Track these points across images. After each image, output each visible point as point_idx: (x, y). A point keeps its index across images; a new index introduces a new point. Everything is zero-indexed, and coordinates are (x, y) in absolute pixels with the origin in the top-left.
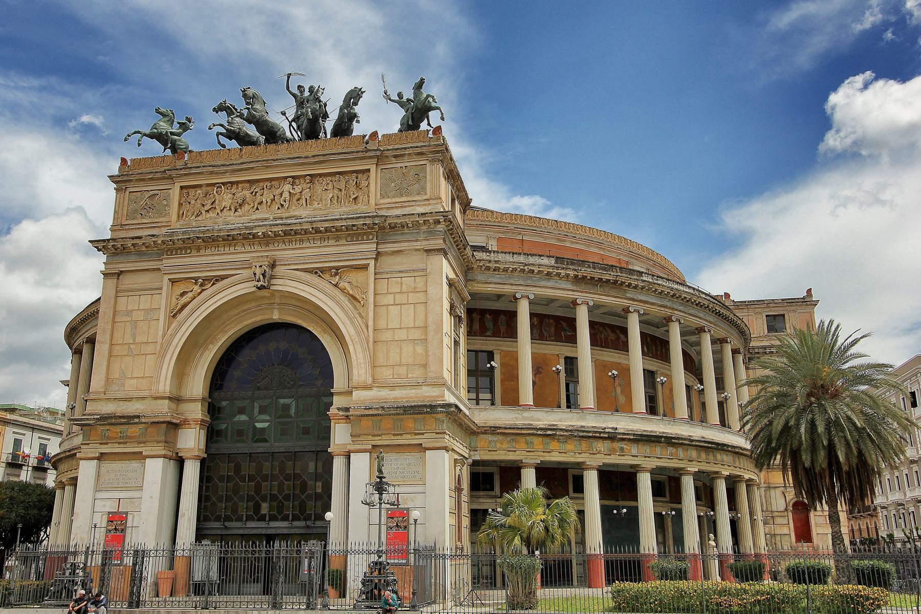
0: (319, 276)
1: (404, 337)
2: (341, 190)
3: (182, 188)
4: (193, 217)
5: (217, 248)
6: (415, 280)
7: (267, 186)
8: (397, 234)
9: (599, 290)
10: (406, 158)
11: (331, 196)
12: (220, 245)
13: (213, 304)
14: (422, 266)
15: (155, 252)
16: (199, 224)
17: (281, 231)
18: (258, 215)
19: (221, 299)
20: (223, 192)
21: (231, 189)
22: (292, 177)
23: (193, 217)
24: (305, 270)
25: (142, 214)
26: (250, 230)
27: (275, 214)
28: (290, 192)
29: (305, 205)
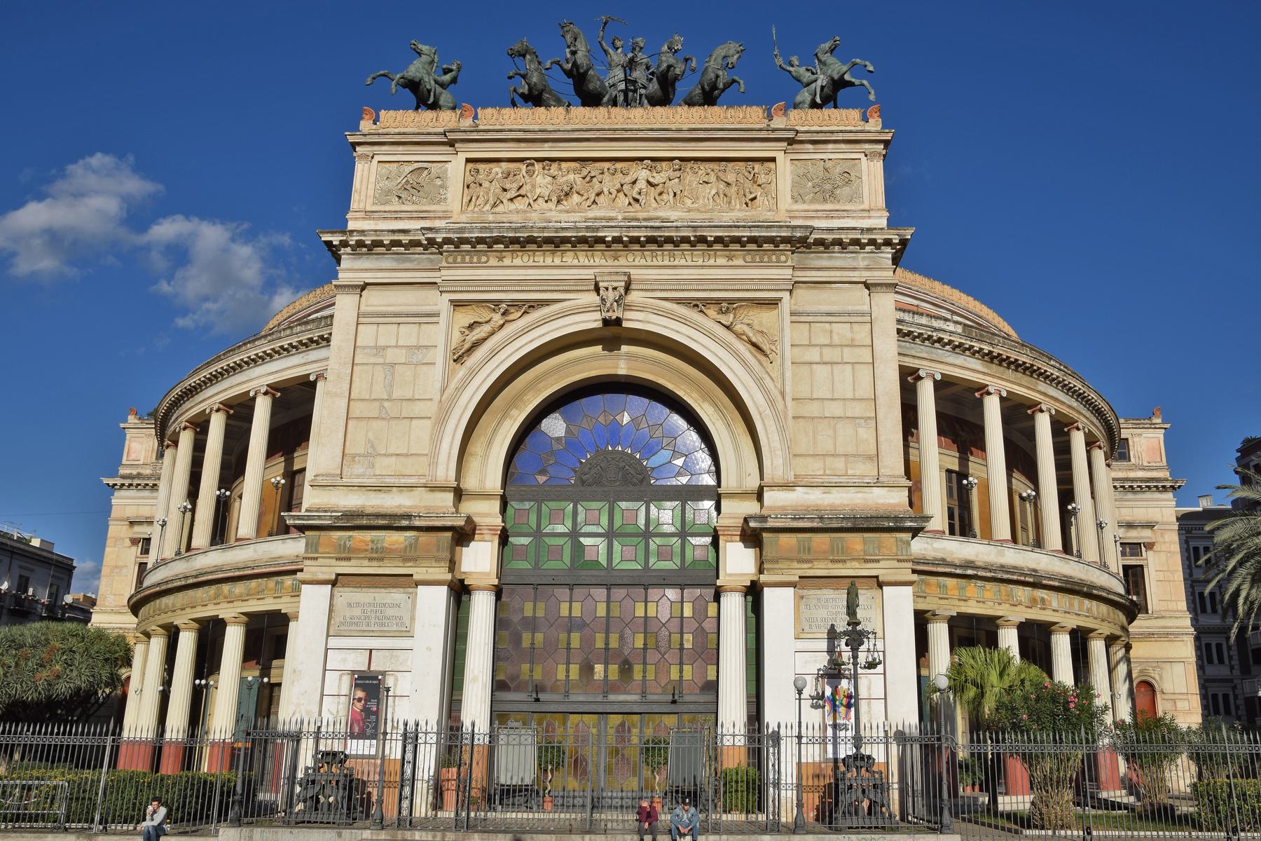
0: (701, 311)
1: (839, 413)
3: (468, 160)
4: (488, 207)
5: (532, 258)
6: (851, 328)
8: (821, 258)
9: (1010, 374)
10: (830, 146)
11: (714, 192)
12: (537, 253)
13: (526, 344)
14: (866, 308)
15: (425, 256)
16: (499, 218)
17: (644, 236)
18: (595, 212)
19: (540, 336)
20: (536, 173)
22: (653, 159)
23: (488, 207)
24: (679, 301)
25: (399, 197)
26: (593, 232)
27: (626, 212)
28: (648, 182)
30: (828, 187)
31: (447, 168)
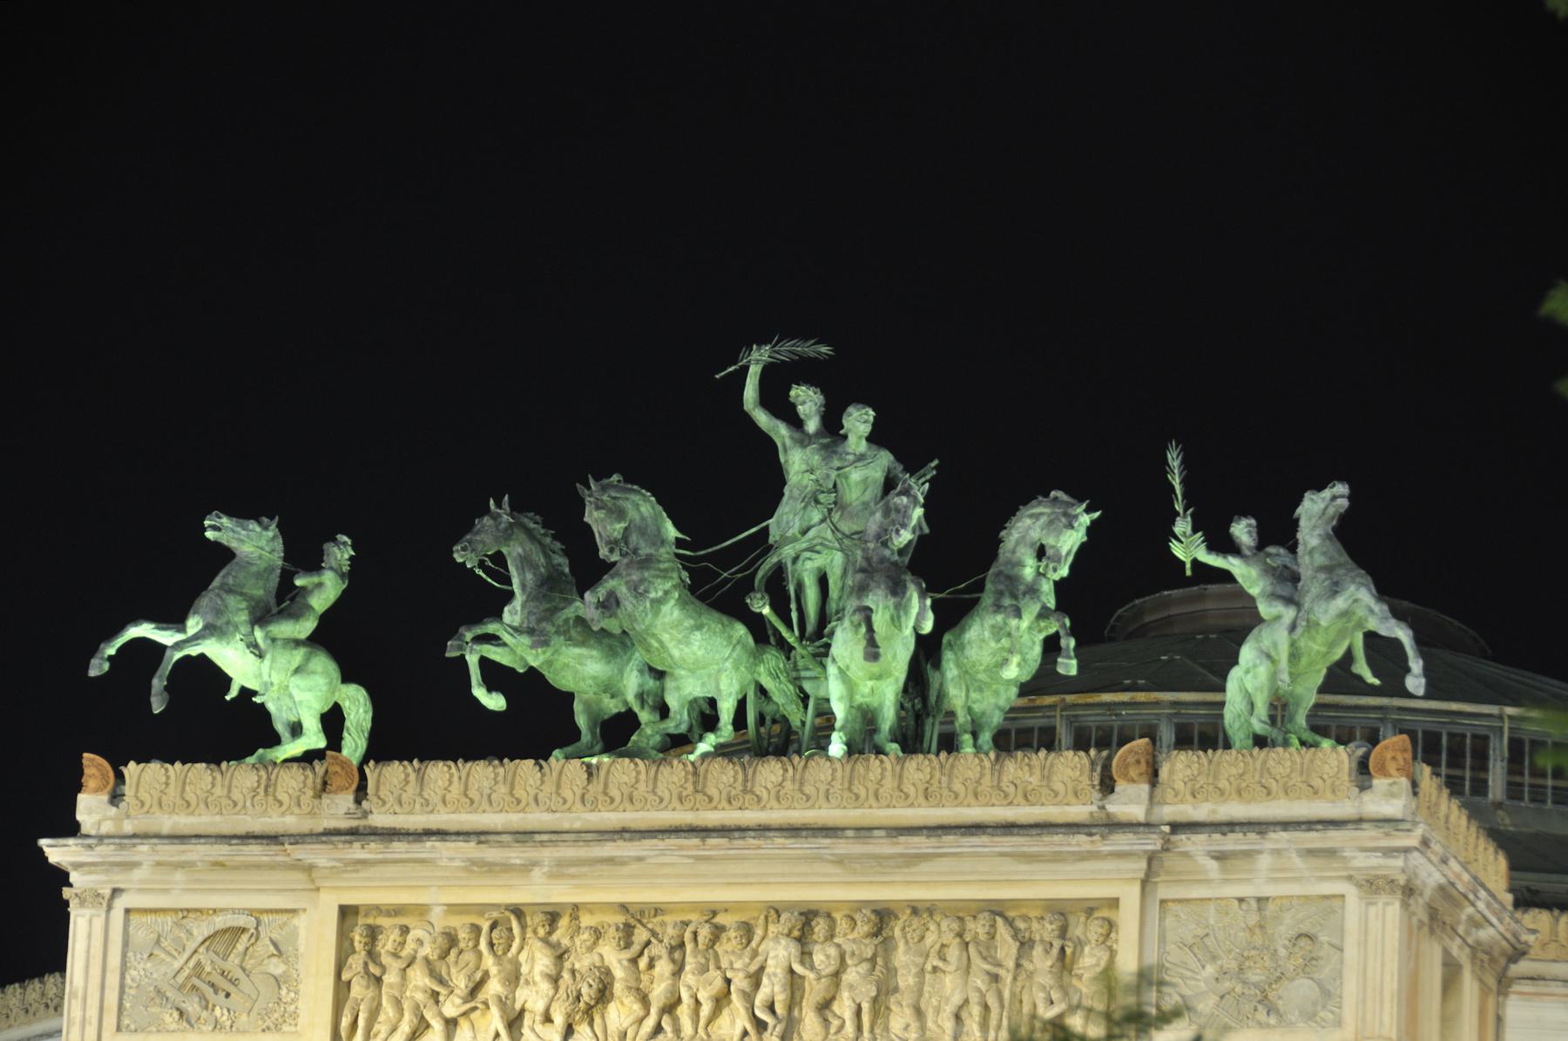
2: (995, 978)
3: (346, 913)
7: (695, 934)
10: (1264, 861)
11: (957, 999)
21: (550, 933)
29: (850, 1028)
30: (1255, 976)
31: (296, 928)
